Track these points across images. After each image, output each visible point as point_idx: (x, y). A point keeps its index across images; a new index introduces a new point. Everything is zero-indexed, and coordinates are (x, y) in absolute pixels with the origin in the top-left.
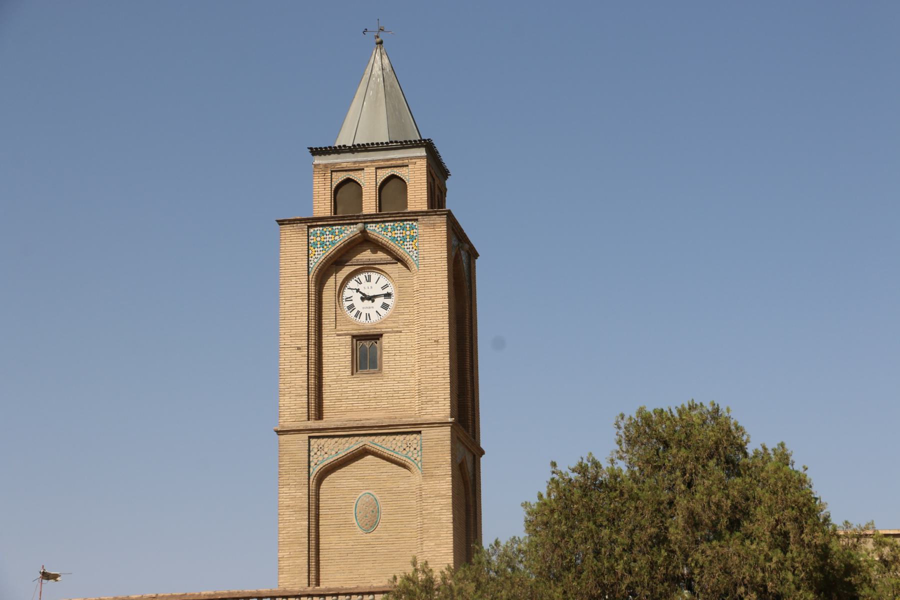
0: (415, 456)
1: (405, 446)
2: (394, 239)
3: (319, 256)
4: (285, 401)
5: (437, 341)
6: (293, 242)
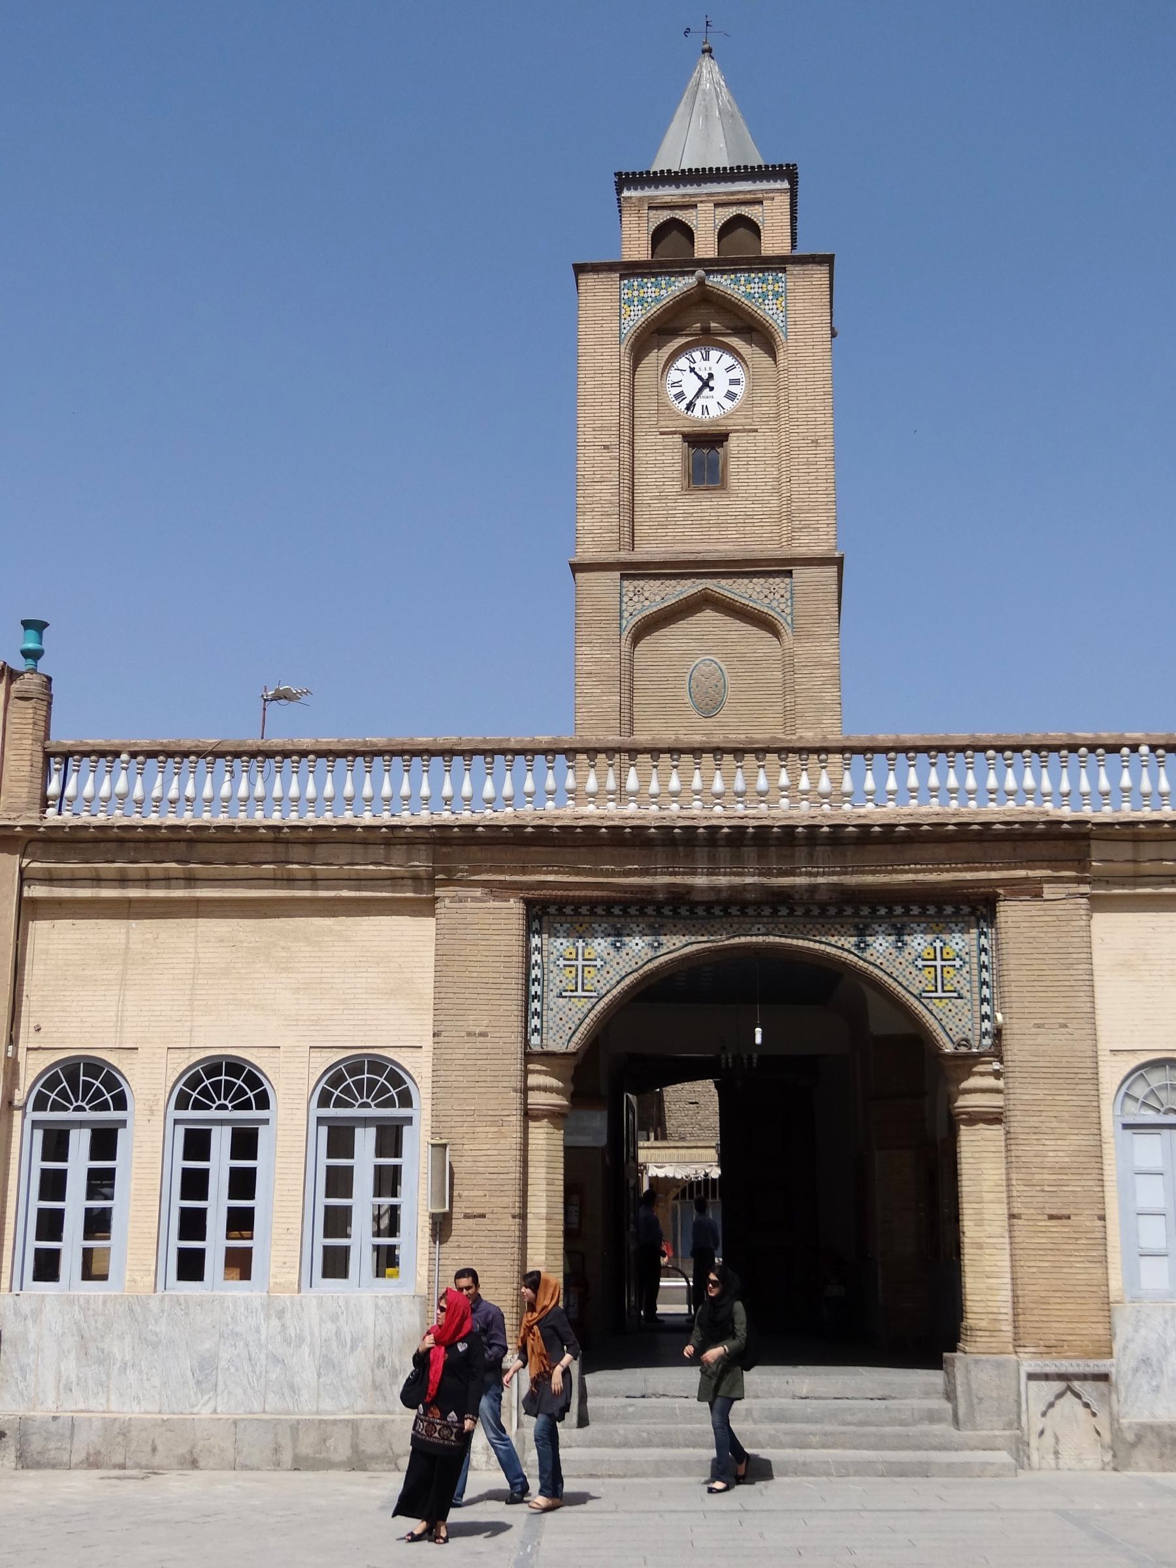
0: (783, 606)
1: (766, 592)
2: (749, 296)
3: (636, 317)
4: (585, 522)
5: (815, 442)
6: (599, 294)
